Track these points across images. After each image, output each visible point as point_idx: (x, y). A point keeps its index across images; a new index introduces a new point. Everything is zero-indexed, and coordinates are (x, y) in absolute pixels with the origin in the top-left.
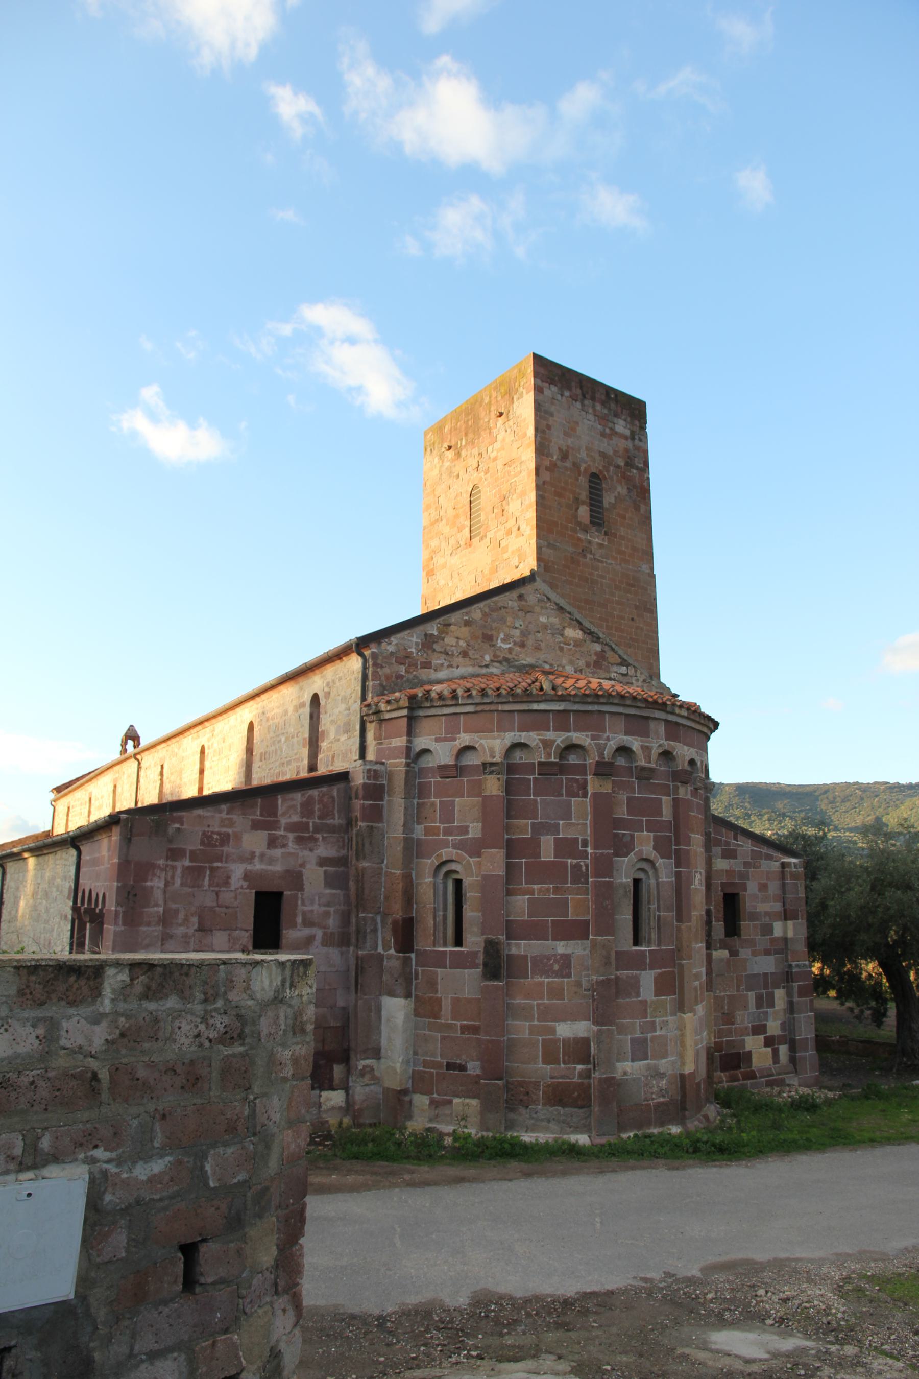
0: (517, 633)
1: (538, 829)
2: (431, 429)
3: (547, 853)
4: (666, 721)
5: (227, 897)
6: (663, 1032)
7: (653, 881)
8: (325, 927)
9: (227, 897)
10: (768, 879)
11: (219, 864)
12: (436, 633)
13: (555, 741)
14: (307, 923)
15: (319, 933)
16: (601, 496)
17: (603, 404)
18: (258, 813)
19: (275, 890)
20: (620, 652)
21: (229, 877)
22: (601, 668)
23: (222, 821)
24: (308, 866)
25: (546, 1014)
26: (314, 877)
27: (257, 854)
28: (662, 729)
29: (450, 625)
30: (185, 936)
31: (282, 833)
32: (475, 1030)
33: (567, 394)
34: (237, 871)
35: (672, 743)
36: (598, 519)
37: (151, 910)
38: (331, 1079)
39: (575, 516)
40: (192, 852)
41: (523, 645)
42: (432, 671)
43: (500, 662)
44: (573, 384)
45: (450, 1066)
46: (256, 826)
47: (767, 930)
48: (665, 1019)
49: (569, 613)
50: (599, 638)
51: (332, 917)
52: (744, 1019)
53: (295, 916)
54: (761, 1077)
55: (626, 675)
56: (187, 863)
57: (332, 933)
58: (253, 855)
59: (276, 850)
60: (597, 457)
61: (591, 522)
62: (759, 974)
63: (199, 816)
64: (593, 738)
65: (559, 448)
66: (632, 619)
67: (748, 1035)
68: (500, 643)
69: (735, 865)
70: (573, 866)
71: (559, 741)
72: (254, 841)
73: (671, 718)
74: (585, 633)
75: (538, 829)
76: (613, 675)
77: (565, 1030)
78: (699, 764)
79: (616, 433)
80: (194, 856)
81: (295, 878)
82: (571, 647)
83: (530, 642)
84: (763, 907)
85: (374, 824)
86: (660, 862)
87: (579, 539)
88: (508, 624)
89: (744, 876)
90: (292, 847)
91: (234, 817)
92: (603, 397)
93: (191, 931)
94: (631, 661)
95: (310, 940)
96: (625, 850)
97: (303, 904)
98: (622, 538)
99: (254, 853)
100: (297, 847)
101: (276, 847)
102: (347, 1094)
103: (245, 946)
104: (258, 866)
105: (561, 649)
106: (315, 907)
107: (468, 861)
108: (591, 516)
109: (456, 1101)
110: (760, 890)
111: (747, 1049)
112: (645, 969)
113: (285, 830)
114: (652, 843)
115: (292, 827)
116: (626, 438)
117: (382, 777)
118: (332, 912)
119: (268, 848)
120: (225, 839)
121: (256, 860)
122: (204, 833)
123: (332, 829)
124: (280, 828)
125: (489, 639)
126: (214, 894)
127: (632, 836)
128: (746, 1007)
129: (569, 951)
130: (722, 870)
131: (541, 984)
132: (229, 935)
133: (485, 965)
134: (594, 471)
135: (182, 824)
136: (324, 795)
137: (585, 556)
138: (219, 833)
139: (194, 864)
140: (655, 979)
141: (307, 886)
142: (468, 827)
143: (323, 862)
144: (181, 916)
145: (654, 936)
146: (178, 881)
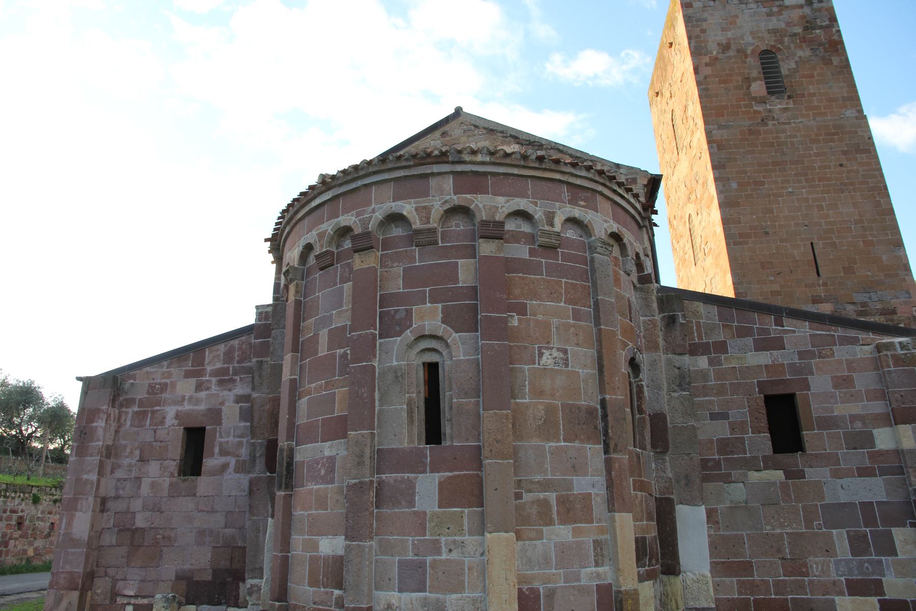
4: (452, 172)
5: (162, 433)
6: (454, 556)
7: (448, 362)
9: (162, 433)
14: (224, 452)
15: (232, 461)
16: (778, 67)
19: (199, 425)
21: (164, 418)
23: (163, 374)
24: (227, 404)
26: (231, 413)
28: (449, 183)
30: (130, 465)
31: (207, 378)
34: (171, 412)
35: (468, 196)
37: (94, 444)
39: (749, 94)
40: (140, 400)
46: (188, 375)
53: (213, 446)
56: (136, 409)
57: (244, 461)
58: (183, 398)
60: (766, 36)
61: (769, 93)
62: (850, 505)
63: (147, 372)
65: (718, 44)
66: (841, 165)
69: (786, 357)
70: (341, 356)
72: (186, 387)
73: (459, 168)
74: (522, 145)
79: (787, 7)
81: (215, 415)
84: (841, 409)
86: (454, 337)
87: (759, 112)
90: (214, 389)
93: (134, 462)
95: (224, 467)
96: (398, 329)
97: (221, 436)
98: (814, 95)
101: (202, 390)
104: (187, 407)
108: (767, 88)
110: (836, 386)
112: (424, 472)
114: (441, 315)
115: (215, 373)
120: (164, 387)
121: (186, 403)
122: (150, 385)
123: (249, 371)
127: (409, 313)
128: (829, 551)
129: (333, 453)
130: (760, 366)
131: (310, 491)
134: (764, 48)
136: (243, 343)
138: (160, 384)
140: (440, 483)
143: (239, 399)
144: (128, 450)
146: (128, 423)
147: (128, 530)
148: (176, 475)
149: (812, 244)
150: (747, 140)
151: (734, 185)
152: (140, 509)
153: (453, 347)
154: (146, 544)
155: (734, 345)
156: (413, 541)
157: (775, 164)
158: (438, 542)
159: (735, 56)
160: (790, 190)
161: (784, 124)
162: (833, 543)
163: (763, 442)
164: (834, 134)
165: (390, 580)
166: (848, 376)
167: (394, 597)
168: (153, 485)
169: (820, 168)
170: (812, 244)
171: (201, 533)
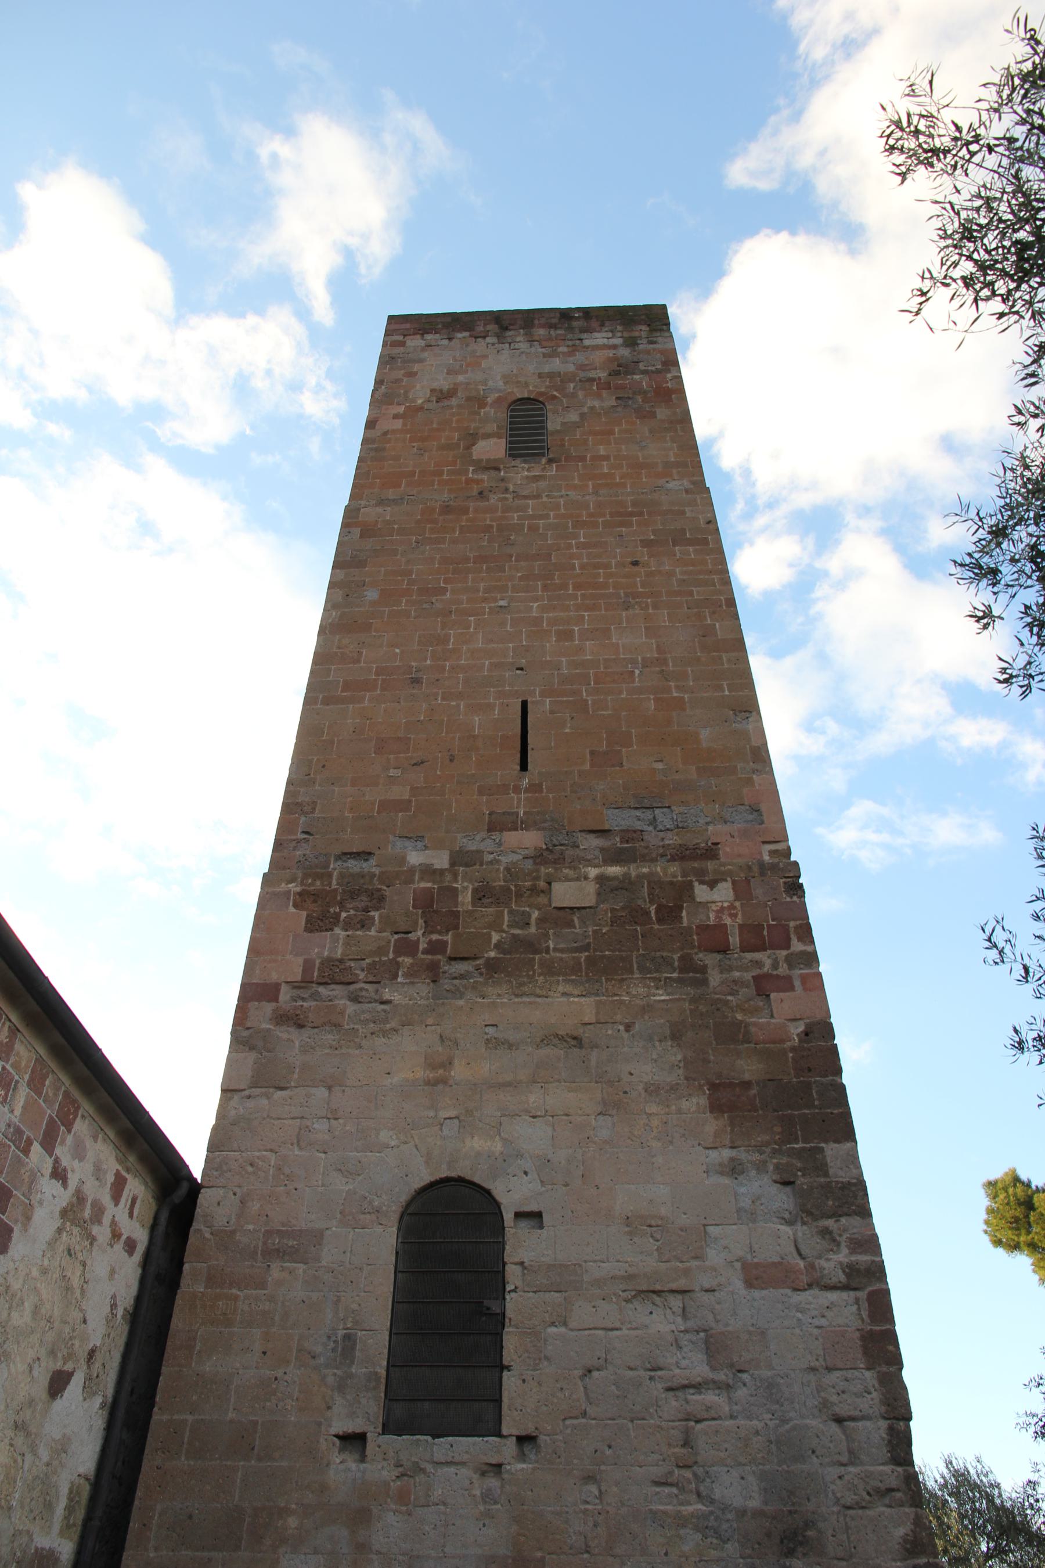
149: (524, 704)
159: (459, 406)
160: (502, 603)
164: (631, 514)
170: (524, 704)
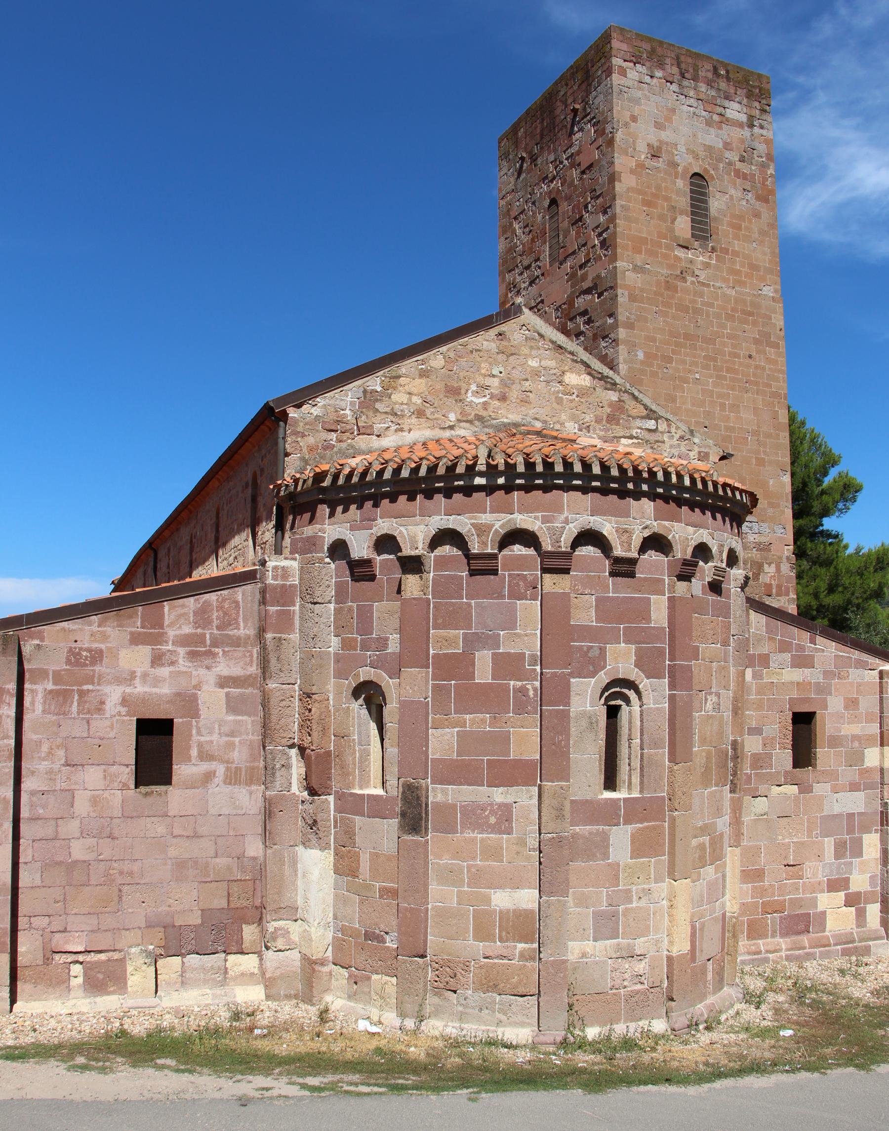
0: (495, 382)
1: (473, 642)
2: (506, 136)
3: (483, 670)
6: (643, 903)
8: (228, 762)
10: (859, 692)
11: (90, 687)
12: (379, 389)
13: (493, 525)
14: (205, 756)
15: (221, 770)
16: (706, 202)
17: (709, 83)
18: (139, 624)
20: (647, 401)
21: (103, 703)
22: (618, 424)
24: (205, 687)
25: (477, 878)
26: (212, 700)
27: (138, 674)
29: (399, 377)
30: (50, 772)
31: (170, 647)
32: (393, 893)
33: (659, 74)
34: (113, 694)
35: (666, 523)
36: (702, 228)
38: (241, 941)
39: (672, 230)
41: (503, 398)
42: (375, 437)
43: (470, 422)
44: (668, 61)
45: (368, 936)
46: (136, 640)
47: (856, 758)
48: (646, 886)
49: (572, 353)
50: (615, 384)
51: (237, 749)
52: (815, 872)
53: (189, 748)
54: (835, 945)
55: (655, 431)
56: (50, 686)
58: (132, 675)
59: (162, 669)
61: (693, 235)
63: (64, 629)
64: (545, 520)
65: (648, 145)
66: (750, 356)
67: (822, 891)
68: (470, 397)
70: (518, 691)
71: (497, 526)
74: (594, 378)
75: (473, 642)
76: (634, 432)
77: (502, 900)
78: (714, 550)
79: (728, 120)
80: (58, 677)
81: (189, 703)
82: (574, 396)
83: (514, 394)
84: (849, 729)
85: (283, 636)
87: (678, 259)
88: (483, 371)
89: (823, 690)
90: (183, 664)
91: (108, 630)
92: (710, 75)
94: (662, 412)
95: (208, 777)
96: (591, 668)
98: (736, 254)
99: (135, 672)
100: (190, 664)
101: (163, 665)
102: (261, 960)
103: (125, 785)
104: (140, 688)
105: (559, 401)
106: (215, 737)
107: (388, 682)
108: (693, 228)
109: (375, 977)
111: (820, 908)
112: (617, 824)
113: (173, 644)
114: (634, 658)
116: (741, 125)
117: (293, 576)
118: (237, 744)
119: (152, 667)
120: (97, 656)
121: (137, 681)
122: (70, 650)
124: (167, 642)
125: (454, 392)
126: (85, 722)
127: (603, 650)
129: (510, 799)
130: (792, 683)
132: (105, 771)
133: (403, 815)
134: (697, 170)
135: (42, 640)
136: (224, 600)
137: (684, 280)
138: (89, 650)
139: (58, 687)
140: (632, 835)
141: (203, 712)
142: (387, 639)
143: (224, 682)
144: (45, 748)
145: (636, 779)
146: (39, 708)
147: (60, 863)
148: (133, 786)
150: (662, 295)
151: (641, 355)
152: (78, 835)
153: (644, 694)
154: (93, 882)
155: (777, 659)
156: (607, 892)
157: (687, 336)
158: (630, 891)
160: (697, 376)
161: (703, 284)
162: (824, 849)
163: (784, 757)
165: (584, 930)
166: (856, 699)
167: (589, 946)
168: (95, 801)
169: (730, 354)
171: (181, 865)
